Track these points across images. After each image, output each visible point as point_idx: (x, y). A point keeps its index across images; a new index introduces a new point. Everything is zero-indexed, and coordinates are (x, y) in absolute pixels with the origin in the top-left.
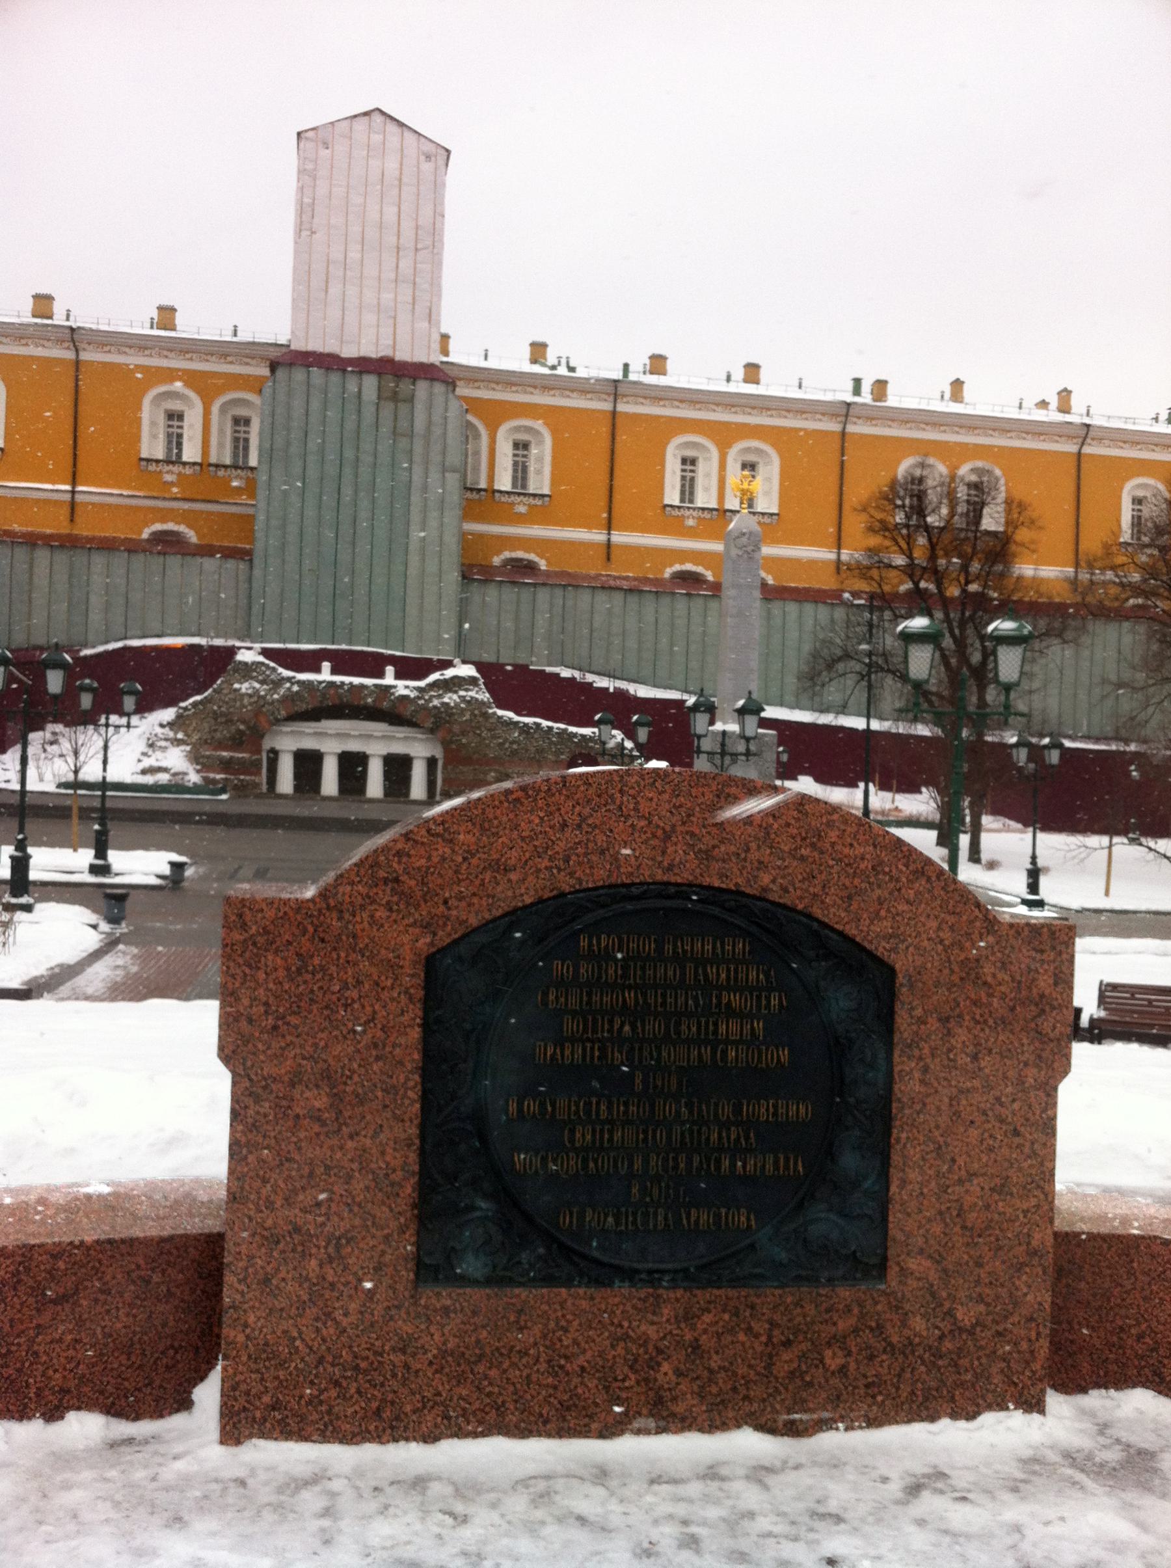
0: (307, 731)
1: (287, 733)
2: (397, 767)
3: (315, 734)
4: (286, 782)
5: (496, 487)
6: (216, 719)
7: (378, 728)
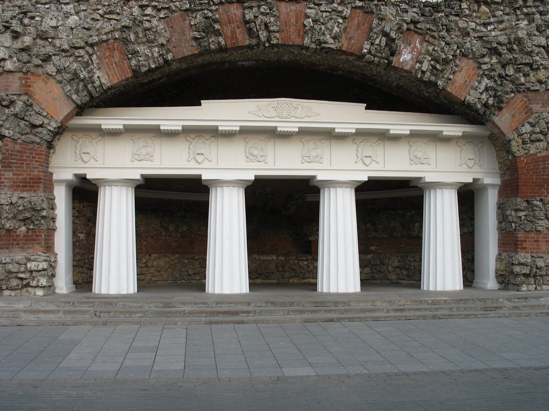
0: (165, 126)
1: (114, 134)
2: (391, 214)
3: (190, 132)
4: (117, 265)
7: (347, 115)
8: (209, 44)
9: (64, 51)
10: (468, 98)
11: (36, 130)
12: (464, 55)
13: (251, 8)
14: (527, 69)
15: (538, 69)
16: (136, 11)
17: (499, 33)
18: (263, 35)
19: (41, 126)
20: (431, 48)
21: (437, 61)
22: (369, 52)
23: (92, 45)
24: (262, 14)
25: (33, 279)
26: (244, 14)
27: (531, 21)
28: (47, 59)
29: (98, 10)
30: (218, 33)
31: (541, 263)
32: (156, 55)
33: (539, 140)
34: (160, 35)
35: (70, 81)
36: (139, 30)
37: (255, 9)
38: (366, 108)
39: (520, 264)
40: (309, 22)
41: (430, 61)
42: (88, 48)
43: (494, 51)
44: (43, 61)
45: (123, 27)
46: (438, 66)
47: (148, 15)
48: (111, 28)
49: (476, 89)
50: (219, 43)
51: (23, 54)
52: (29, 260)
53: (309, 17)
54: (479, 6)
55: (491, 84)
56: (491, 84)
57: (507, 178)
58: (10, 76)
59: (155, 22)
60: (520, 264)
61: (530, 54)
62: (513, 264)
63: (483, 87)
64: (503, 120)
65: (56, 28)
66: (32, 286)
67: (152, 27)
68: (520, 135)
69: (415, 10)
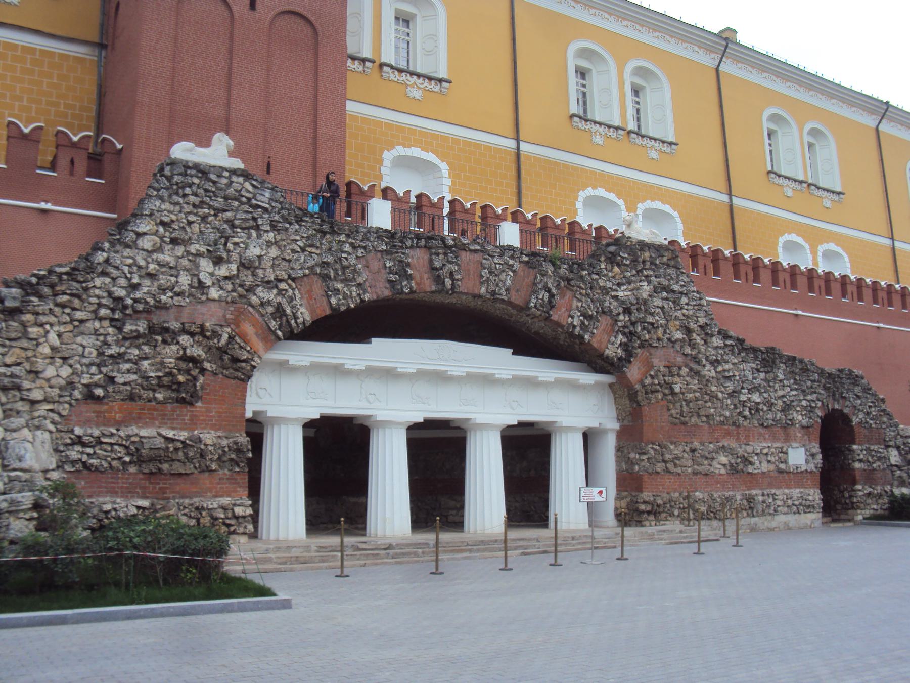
0: (350, 365)
3: (372, 373)
5: (383, 60)
6: (118, 325)
7: (498, 360)
8: (402, 287)
9: (269, 282)
10: (607, 351)
11: (239, 364)
12: (604, 312)
13: (438, 254)
14: (650, 327)
15: (658, 327)
16: (335, 246)
17: (629, 293)
18: (448, 282)
19: (244, 361)
20: (580, 304)
21: (585, 317)
22: (535, 306)
23: (293, 280)
24: (448, 261)
25: (239, 524)
26: (431, 261)
27: (649, 283)
28: (251, 290)
29: (297, 241)
30: (409, 278)
31: (660, 502)
32: (354, 294)
33: (658, 391)
34: (359, 274)
35: (273, 316)
36: (338, 266)
37: (441, 256)
38: (513, 354)
39: (645, 502)
40: (485, 272)
41: (579, 317)
42: (290, 282)
43: (627, 311)
44: (247, 291)
45: (324, 263)
46: (586, 323)
47: (345, 252)
48: (313, 263)
49: (613, 344)
50: (411, 288)
51: (227, 282)
52: (235, 505)
53: (485, 268)
54: (613, 266)
55: (625, 340)
56: (625, 340)
57: (626, 423)
58: (214, 307)
59: (353, 261)
60: (645, 502)
61: (652, 314)
62: (637, 502)
63: (619, 342)
64: (633, 372)
65: (260, 257)
66: (238, 534)
67: (350, 265)
68: (644, 386)
69: (565, 266)
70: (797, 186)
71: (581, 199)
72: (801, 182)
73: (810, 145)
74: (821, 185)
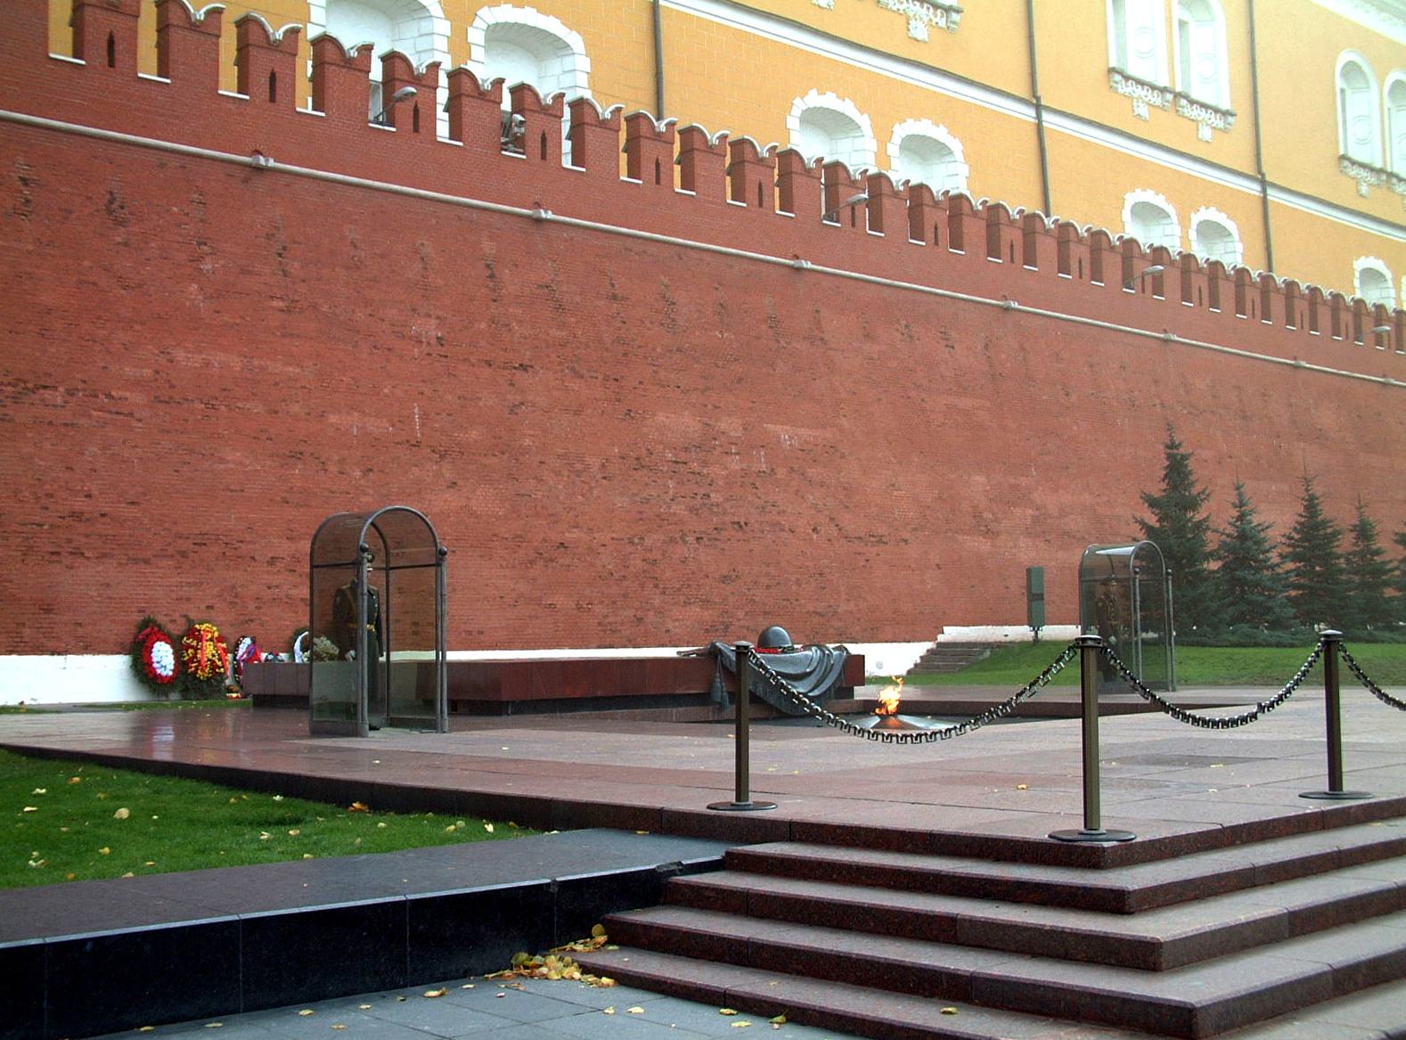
70: (1156, 98)
71: (797, 111)
72: (1163, 90)
73: (1182, 24)
74: (1194, 96)
